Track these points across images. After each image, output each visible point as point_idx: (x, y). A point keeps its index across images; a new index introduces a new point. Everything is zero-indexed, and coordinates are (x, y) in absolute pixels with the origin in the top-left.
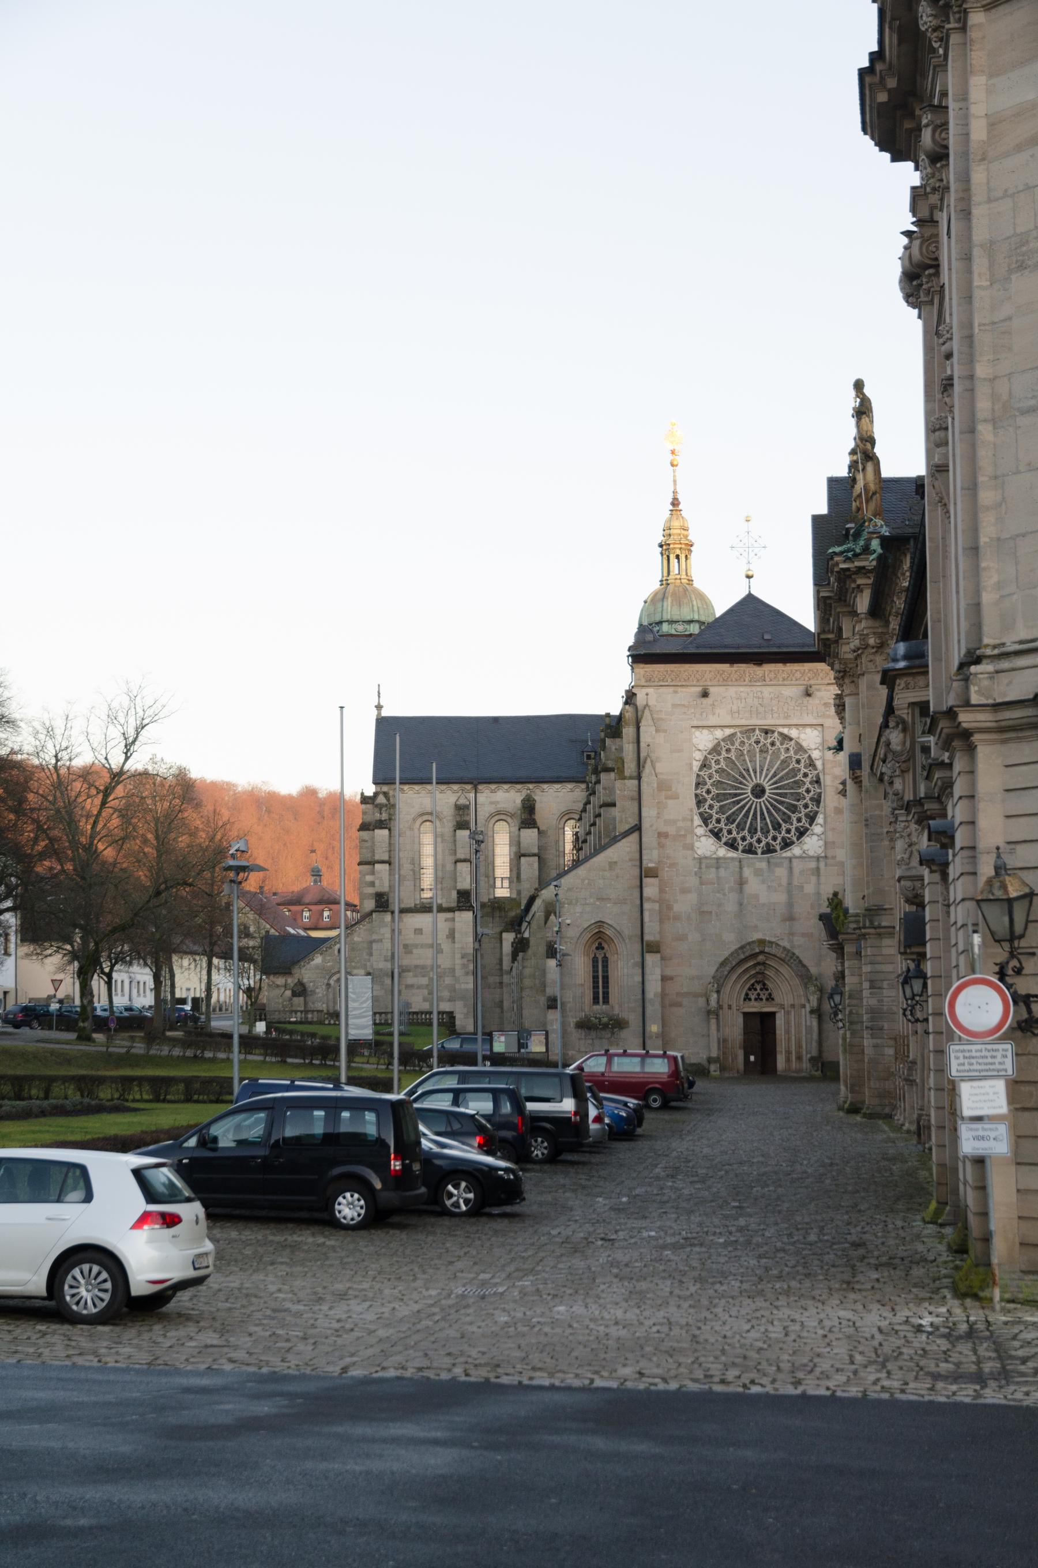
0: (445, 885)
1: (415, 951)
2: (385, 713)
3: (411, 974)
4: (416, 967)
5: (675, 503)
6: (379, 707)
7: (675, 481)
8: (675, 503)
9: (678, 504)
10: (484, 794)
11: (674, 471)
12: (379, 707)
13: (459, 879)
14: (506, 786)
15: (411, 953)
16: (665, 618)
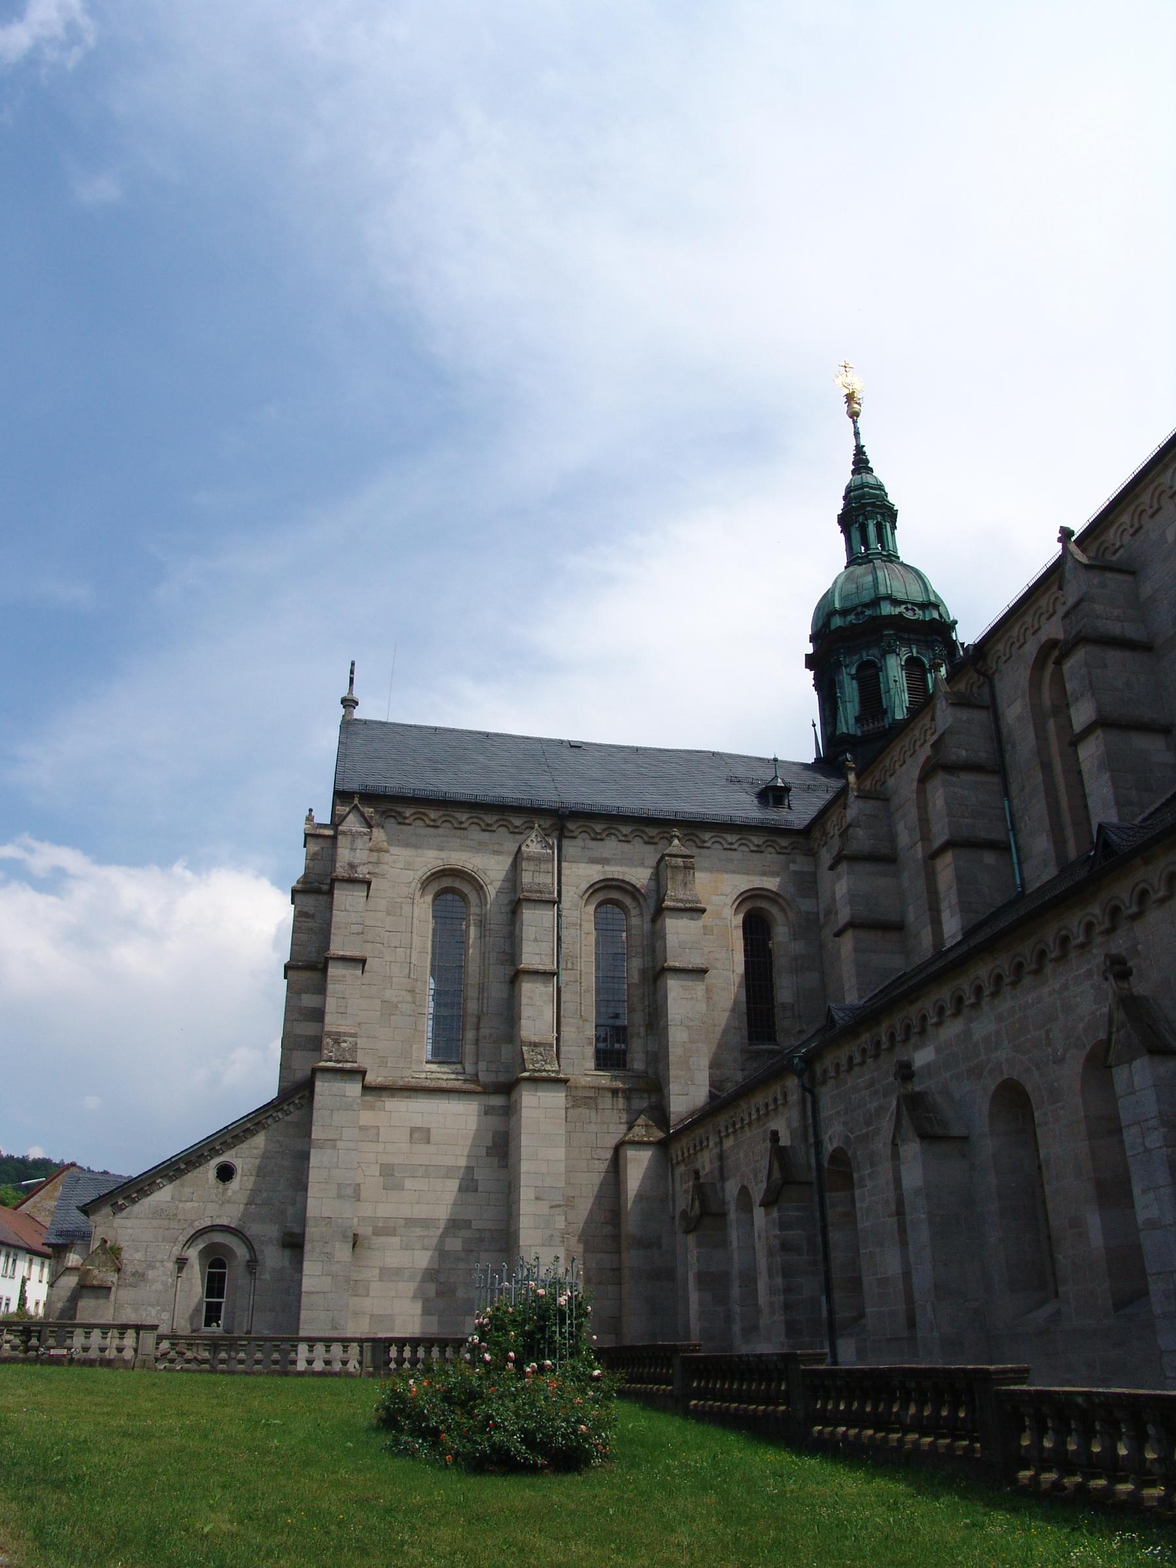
0: (485, 1031)
1: (409, 1184)
2: (358, 714)
3: (395, 1240)
4: (410, 1222)
5: (861, 463)
6: (349, 703)
7: (857, 434)
8: (861, 463)
9: (867, 461)
10: (579, 842)
11: (855, 422)
12: (349, 703)
13: (526, 1012)
14: (626, 830)
15: (401, 1188)
16: (882, 590)
